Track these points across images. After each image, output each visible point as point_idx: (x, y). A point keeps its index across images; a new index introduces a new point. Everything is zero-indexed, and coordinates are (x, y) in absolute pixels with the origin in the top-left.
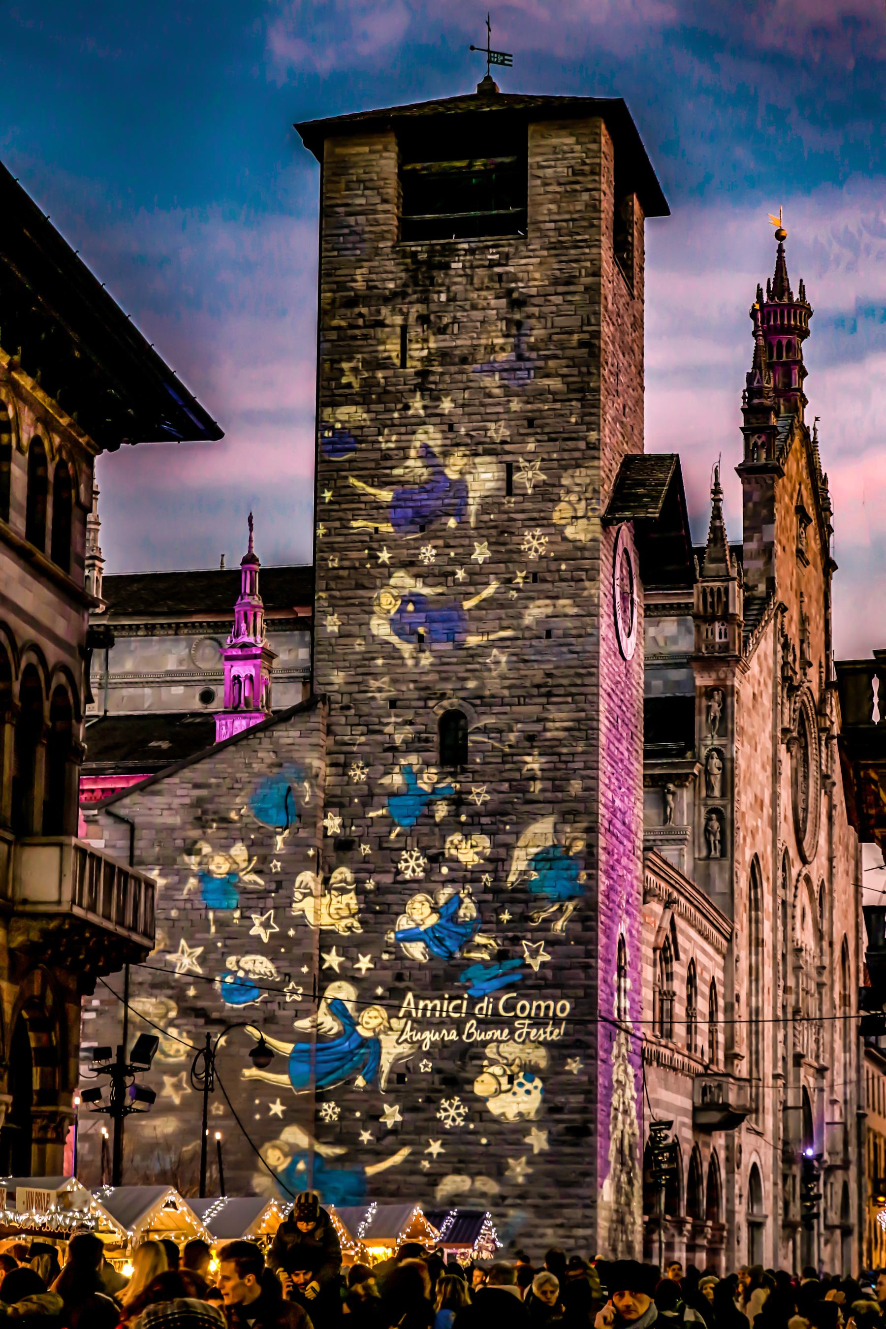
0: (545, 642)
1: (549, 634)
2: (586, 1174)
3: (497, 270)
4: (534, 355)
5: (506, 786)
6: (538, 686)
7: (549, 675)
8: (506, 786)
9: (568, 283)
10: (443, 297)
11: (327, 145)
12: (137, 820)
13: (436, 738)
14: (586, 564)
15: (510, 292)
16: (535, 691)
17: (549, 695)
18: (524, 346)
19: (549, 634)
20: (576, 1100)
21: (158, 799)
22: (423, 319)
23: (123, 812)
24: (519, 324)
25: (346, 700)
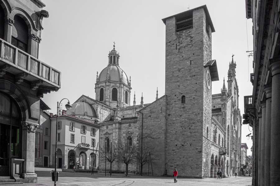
0: (196, 84)
1: (196, 83)
2: (201, 158)
3: (189, 34)
4: (194, 45)
5: (190, 105)
6: (195, 91)
7: (196, 89)
8: (190, 105)
9: (199, 33)
10: (182, 39)
11: (166, 22)
12: (143, 113)
13: (181, 100)
14: (202, 73)
15: (191, 36)
16: (194, 92)
17: (196, 92)
18: (193, 43)
19: (196, 83)
20: (200, 148)
21: (146, 110)
22: (179, 42)
23: (142, 112)
24: (192, 41)
25: (169, 95)
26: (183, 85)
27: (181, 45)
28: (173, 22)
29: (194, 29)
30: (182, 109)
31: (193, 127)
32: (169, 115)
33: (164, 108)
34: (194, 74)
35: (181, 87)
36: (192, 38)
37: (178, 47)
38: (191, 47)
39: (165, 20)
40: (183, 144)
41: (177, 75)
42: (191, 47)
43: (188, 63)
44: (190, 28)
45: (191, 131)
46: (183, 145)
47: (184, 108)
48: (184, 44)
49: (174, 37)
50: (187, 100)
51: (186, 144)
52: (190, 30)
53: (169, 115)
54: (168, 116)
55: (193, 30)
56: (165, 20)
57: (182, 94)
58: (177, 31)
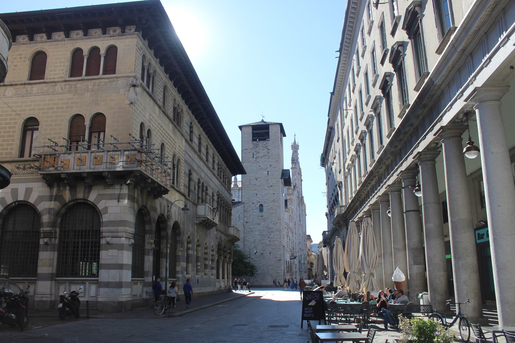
22: (256, 152)
26: (261, 194)
27: (258, 155)
28: (250, 130)
29: (270, 141)
30: (260, 218)
31: (272, 236)
32: (247, 222)
33: (242, 216)
34: (271, 184)
35: (259, 195)
36: (269, 150)
37: (255, 156)
38: (268, 158)
39: (241, 127)
40: (262, 252)
41: (254, 183)
42: (268, 158)
43: (266, 173)
44: (265, 140)
45: (270, 240)
46: (262, 254)
47: (262, 216)
48: (261, 155)
49: (251, 146)
50: (265, 209)
51: (265, 252)
52: (267, 142)
53: (247, 222)
54: (245, 224)
55: (269, 143)
56: (241, 127)
57: (259, 202)
58: (253, 140)
